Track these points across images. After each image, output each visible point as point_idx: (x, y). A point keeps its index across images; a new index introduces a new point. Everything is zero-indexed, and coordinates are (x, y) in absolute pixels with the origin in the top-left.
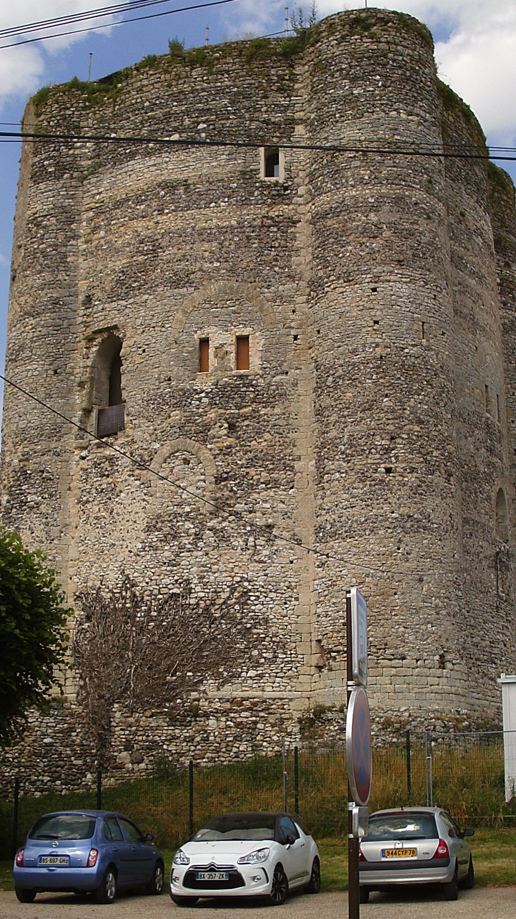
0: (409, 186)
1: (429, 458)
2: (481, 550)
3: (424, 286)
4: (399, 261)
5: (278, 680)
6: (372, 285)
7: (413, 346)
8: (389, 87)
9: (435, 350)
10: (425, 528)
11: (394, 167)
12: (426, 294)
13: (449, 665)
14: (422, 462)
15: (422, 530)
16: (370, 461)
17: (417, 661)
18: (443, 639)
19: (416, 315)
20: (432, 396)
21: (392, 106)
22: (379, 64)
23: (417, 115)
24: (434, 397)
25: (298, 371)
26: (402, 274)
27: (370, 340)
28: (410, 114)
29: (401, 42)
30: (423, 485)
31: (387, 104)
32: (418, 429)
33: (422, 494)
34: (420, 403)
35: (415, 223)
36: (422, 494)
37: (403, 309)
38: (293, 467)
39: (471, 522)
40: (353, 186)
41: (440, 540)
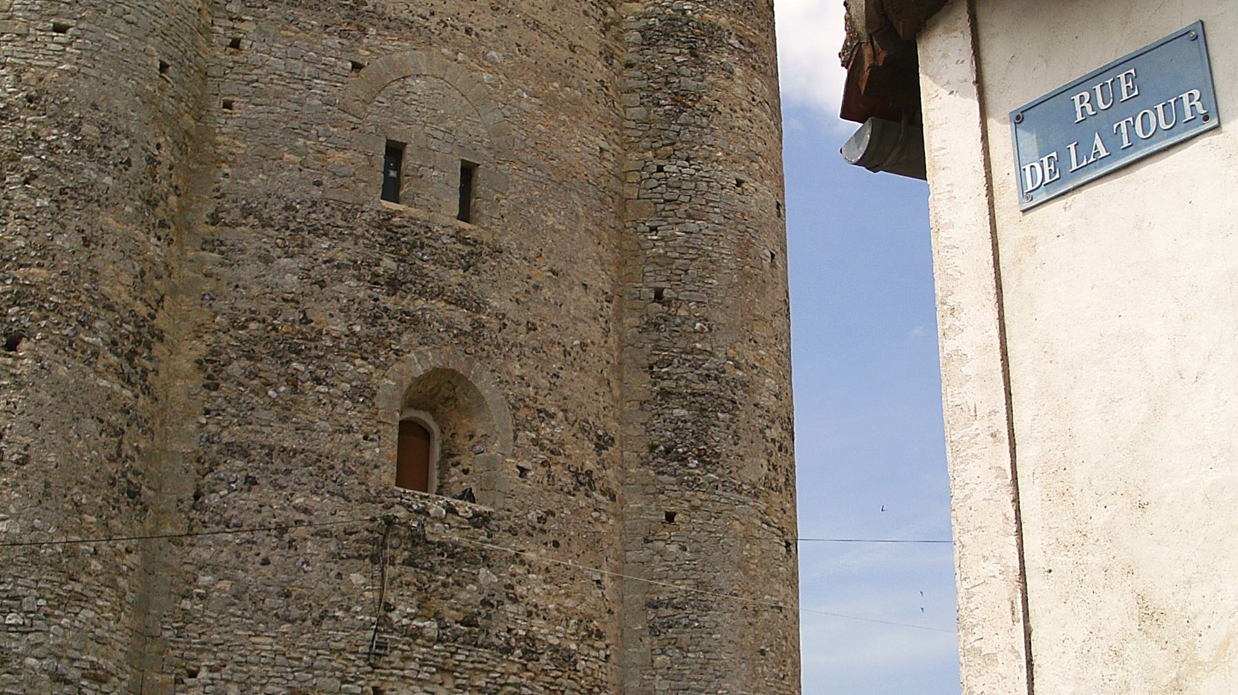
9: (13, 65)
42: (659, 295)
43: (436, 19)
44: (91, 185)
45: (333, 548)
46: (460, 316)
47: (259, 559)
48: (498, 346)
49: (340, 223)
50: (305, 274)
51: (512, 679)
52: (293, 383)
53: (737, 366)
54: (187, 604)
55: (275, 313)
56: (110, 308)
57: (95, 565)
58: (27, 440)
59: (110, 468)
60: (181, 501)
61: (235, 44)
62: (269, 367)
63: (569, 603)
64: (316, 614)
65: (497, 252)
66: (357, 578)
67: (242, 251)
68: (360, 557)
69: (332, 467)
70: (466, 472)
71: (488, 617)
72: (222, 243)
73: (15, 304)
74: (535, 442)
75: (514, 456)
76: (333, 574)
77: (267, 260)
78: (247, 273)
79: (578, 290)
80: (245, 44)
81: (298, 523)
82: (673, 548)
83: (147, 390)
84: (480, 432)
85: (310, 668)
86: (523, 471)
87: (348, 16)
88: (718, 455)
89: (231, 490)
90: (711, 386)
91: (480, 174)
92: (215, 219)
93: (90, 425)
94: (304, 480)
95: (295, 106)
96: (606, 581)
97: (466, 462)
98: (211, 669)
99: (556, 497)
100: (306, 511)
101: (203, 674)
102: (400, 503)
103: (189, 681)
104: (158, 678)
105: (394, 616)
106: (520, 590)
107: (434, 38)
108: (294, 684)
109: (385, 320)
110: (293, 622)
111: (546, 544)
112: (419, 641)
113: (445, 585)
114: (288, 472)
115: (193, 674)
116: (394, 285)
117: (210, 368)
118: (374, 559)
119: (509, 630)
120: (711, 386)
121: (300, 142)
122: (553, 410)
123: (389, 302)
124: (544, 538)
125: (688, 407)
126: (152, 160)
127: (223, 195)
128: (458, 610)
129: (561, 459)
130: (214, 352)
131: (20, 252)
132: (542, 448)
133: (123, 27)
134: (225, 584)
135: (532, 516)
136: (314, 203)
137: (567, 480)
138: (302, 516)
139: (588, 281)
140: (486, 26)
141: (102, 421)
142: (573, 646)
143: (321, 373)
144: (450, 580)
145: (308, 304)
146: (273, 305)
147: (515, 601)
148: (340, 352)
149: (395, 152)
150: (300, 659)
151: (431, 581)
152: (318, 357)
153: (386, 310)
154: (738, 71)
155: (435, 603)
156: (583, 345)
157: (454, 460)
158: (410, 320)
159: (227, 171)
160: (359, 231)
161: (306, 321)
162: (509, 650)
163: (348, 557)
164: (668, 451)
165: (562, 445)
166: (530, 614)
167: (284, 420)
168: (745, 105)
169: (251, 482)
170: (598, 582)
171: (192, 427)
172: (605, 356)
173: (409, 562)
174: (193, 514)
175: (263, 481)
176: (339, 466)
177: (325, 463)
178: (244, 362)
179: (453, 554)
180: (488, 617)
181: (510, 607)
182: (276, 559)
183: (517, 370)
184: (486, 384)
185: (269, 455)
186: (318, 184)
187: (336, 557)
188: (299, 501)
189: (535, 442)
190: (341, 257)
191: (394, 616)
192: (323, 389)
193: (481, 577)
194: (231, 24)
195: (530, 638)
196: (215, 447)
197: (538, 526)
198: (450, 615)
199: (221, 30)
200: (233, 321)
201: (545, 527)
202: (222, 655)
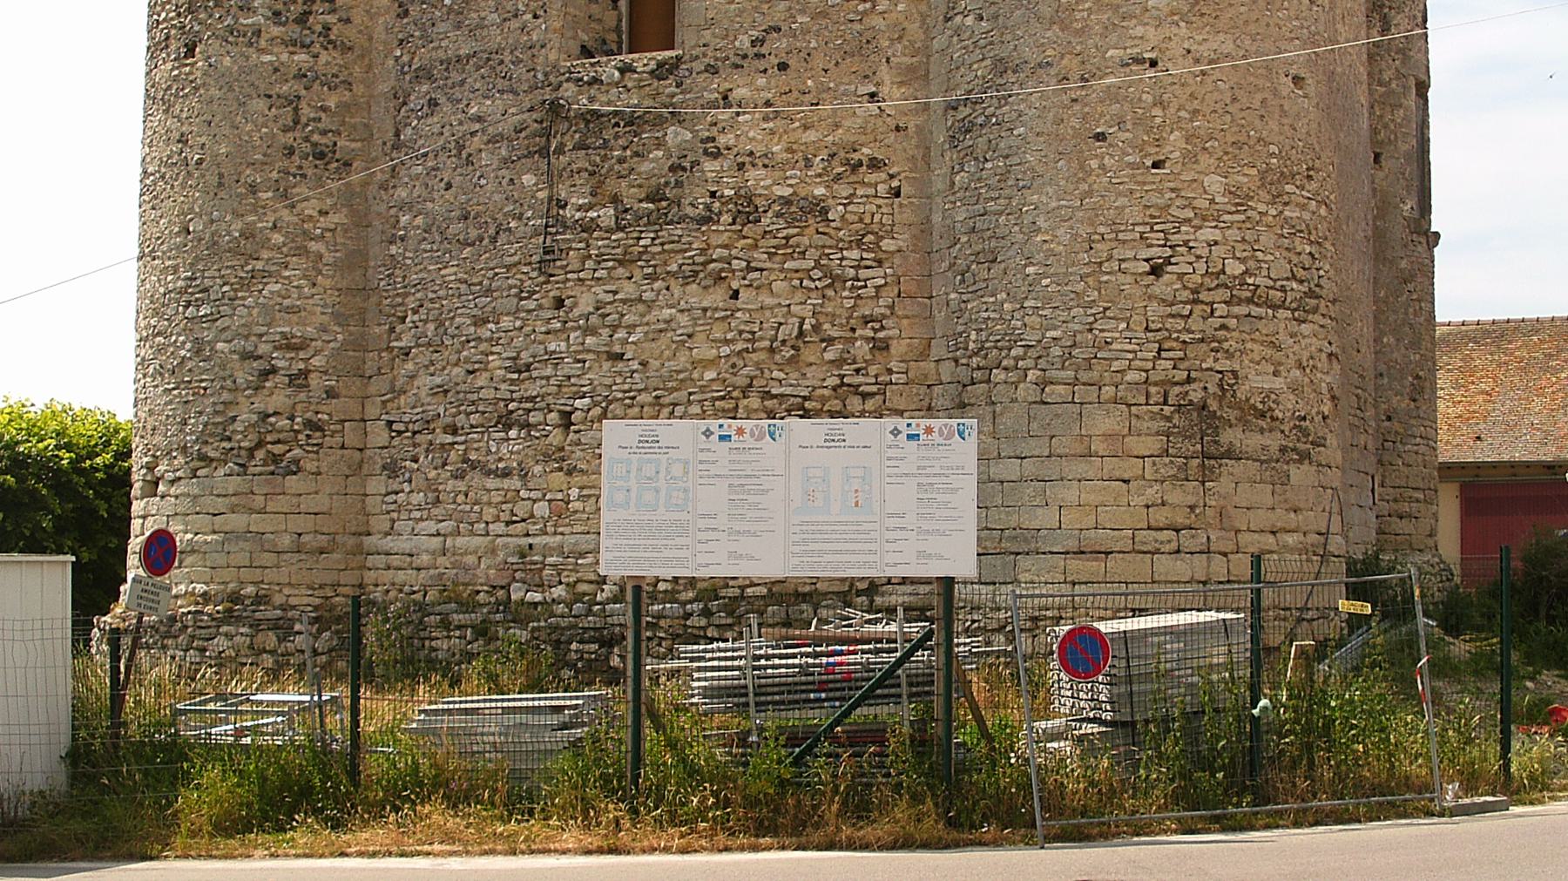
45: (504, 152)
47: (442, 185)
54: (393, 250)
57: (277, 238)
64: (492, 231)
66: (528, 179)
68: (530, 155)
71: (679, 184)
76: (504, 182)
81: (473, 134)
82: (969, 21)
85: (488, 292)
93: (260, 105)
100: (479, 119)
102: (568, 80)
106: (722, 140)
108: (475, 312)
110: (472, 244)
111: (765, 71)
113: (621, 161)
114: (463, 82)
118: (544, 152)
119: (713, 195)
124: (762, 64)
128: (640, 186)
135: (743, 42)
138: (477, 126)
141: (270, 97)
142: (820, 191)
144: (628, 153)
147: (716, 155)
150: (480, 283)
151: (605, 158)
155: (611, 185)
170: (872, 95)
176: (508, 58)
179: (633, 122)
180: (679, 184)
181: (710, 166)
191: (568, 212)
196: (408, 77)
197: (751, 52)
198: (630, 194)
201: (764, 50)
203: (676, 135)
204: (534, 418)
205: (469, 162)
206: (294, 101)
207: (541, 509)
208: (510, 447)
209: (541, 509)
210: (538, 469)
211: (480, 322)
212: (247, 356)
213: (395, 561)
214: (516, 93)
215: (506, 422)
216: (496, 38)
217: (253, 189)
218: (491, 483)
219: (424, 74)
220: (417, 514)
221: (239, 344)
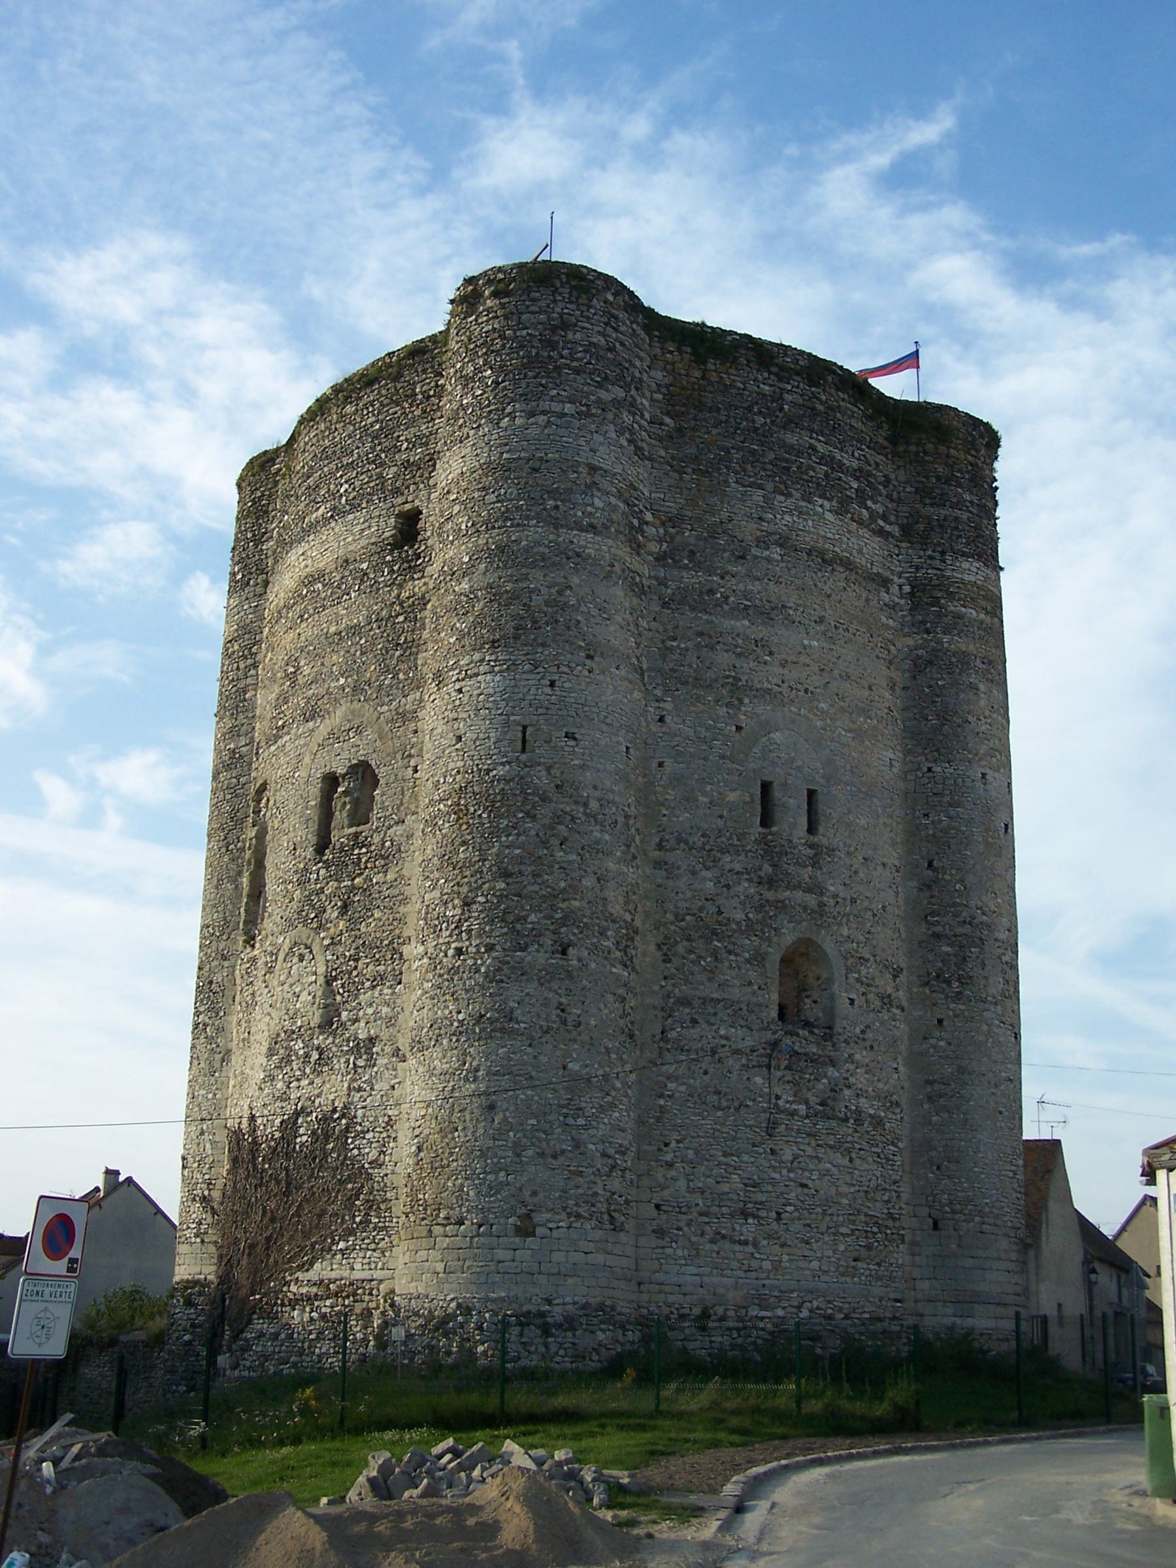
0: (518, 525)
1: (518, 927)
2: (724, 1042)
3: (531, 672)
4: (494, 642)
5: (369, 1253)
6: (457, 686)
7: (503, 764)
8: (503, 381)
10: (503, 1030)
11: (498, 501)
12: (531, 682)
13: (540, 1231)
14: (506, 934)
15: (499, 1035)
16: (441, 941)
17: (480, 1226)
18: (527, 1193)
19: (512, 718)
20: (533, 833)
21: (504, 409)
22: (493, 352)
23: (543, 413)
24: (537, 835)
25: (414, 817)
26: (495, 661)
27: (452, 765)
28: (532, 414)
29: (528, 307)
30: (505, 967)
31: (497, 410)
32: (503, 885)
33: (502, 981)
34: (508, 847)
35: (526, 578)
36: (502, 981)
37: (493, 712)
38: (401, 954)
39: (696, 1003)
40: (452, 543)
41: (530, 1045)
42: (930, 865)
43: (786, 685)
44: (598, 842)
46: (811, 900)
48: (834, 918)
49: (736, 842)
50: (717, 881)
51: (849, 1139)
52: (715, 954)
53: (983, 913)
54: (662, 1102)
55: (701, 909)
56: (614, 921)
58: (579, 1012)
59: (622, 1022)
60: (654, 1036)
61: (661, 719)
62: (700, 944)
63: (880, 1085)
64: (736, 1104)
65: (831, 851)
66: (759, 1080)
67: (679, 868)
68: (760, 1066)
69: (741, 1009)
70: (815, 1002)
72: (666, 863)
73: (564, 926)
74: (858, 980)
75: (846, 991)
77: (694, 873)
78: (682, 883)
79: (880, 868)
80: (668, 719)
81: (723, 1046)
82: (942, 1043)
83: (634, 970)
84: (825, 975)
86: (852, 1001)
87: (731, 691)
88: (971, 978)
89: (682, 1027)
90: (967, 929)
91: (820, 797)
92: (660, 847)
93: (610, 998)
94: (725, 1018)
95: (702, 762)
96: (901, 1069)
97: (815, 995)
98: (678, 1142)
99: (871, 1015)
100: (727, 1038)
101: (673, 1144)
103: (665, 1149)
104: (647, 1148)
105: (780, 1102)
107: (786, 700)
109: (767, 908)
112: (796, 1118)
114: (715, 1014)
115: (666, 1145)
116: (771, 883)
117: (665, 948)
120: (967, 929)
121: (709, 788)
122: (867, 956)
123: (770, 895)
125: (951, 945)
126: (627, 817)
127: (664, 830)
129: (873, 989)
130: (666, 938)
131: (564, 891)
132: (862, 983)
133: (605, 728)
134: (682, 1088)
135: (858, 1030)
136: (720, 831)
137: (878, 1003)
138: (724, 1042)
139: (885, 860)
140: (817, 684)
143: (731, 947)
145: (721, 901)
146: (700, 904)
147: (849, 1087)
148: (741, 932)
149: (766, 787)
152: (729, 937)
153: (768, 901)
154: (982, 687)
156: (884, 907)
157: (808, 993)
158: (781, 906)
159: (665, 812)
160: (749, 847)
161: (720, 913)
162: (846, 1120)
163: (754, 1067)
164: (938, 976)
165: (873, 979)
166: (858, 1095)
167: (710, 980)
168: (987, 713)
169: (695, 1022)
171: (657, 988)
172: (897, 912)
173: (788, 1068)
174: (662, 1044)
175: (701, 1021)
177: (736, 1007)
178: (685, 943)
179: (812, 1060)
181: (847, 1092)
182: (711, 1070)
183: (845, 932)
184: (829, 947)
185: (704, 1004)
186: (721, 817)
187: (746, 1067)
188: (722, 1032)
189: (858, 980)
190: (738, 867)
191: (780, 1102)
192: (732, 957)
193: (829, 1074)
194: (657, 704)
195: (859, 1111)
198: (813, 1100)
199: (652, 710)
200: (676, 916)
202: (683, 1132)
203: (831, 1072)
204: (763, 1213)
205: (719, 1061)
206: (623, 1000)
207: (767, 1265)
208: (748, 1229)
209: (767, 1265)
210: (765, 1242)
211: (725, 1155)
212: (604, 1155)
213: (667, 1289)
214: (751, 1029)
215: (745, 1214)
216: (735, 993)
217: (608, 1051)
218: (737, 1247)
219: (685, 1002)
220: (683, 1262)
221: (600, 1147)
